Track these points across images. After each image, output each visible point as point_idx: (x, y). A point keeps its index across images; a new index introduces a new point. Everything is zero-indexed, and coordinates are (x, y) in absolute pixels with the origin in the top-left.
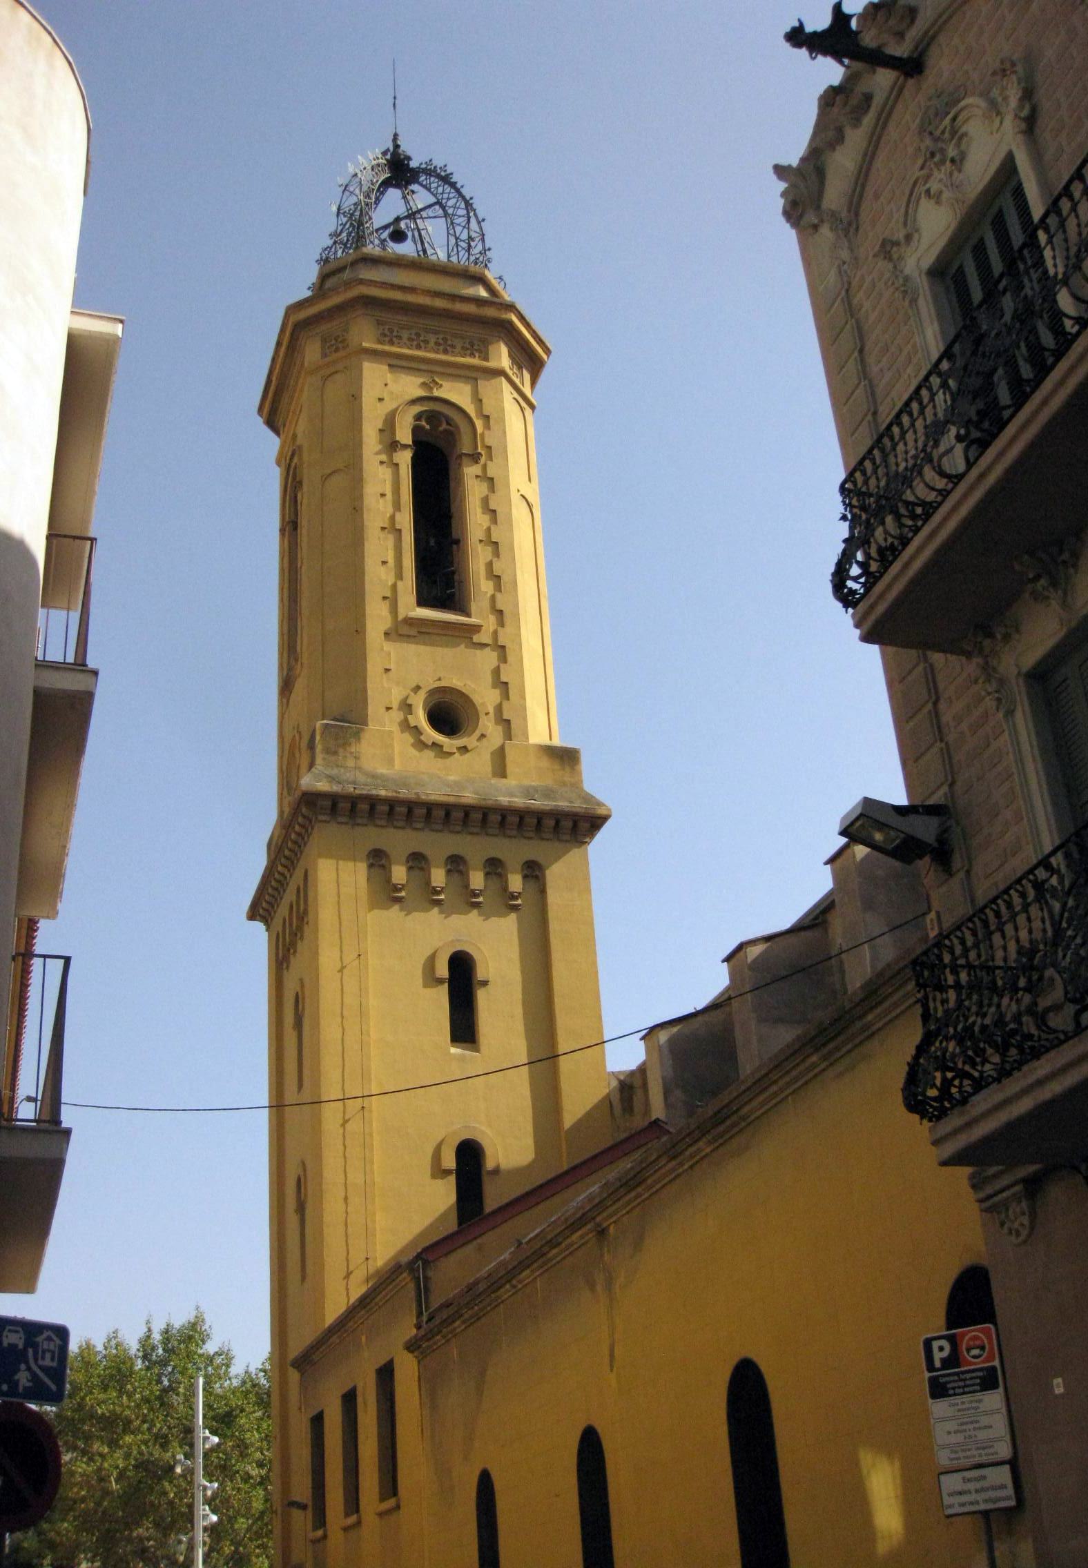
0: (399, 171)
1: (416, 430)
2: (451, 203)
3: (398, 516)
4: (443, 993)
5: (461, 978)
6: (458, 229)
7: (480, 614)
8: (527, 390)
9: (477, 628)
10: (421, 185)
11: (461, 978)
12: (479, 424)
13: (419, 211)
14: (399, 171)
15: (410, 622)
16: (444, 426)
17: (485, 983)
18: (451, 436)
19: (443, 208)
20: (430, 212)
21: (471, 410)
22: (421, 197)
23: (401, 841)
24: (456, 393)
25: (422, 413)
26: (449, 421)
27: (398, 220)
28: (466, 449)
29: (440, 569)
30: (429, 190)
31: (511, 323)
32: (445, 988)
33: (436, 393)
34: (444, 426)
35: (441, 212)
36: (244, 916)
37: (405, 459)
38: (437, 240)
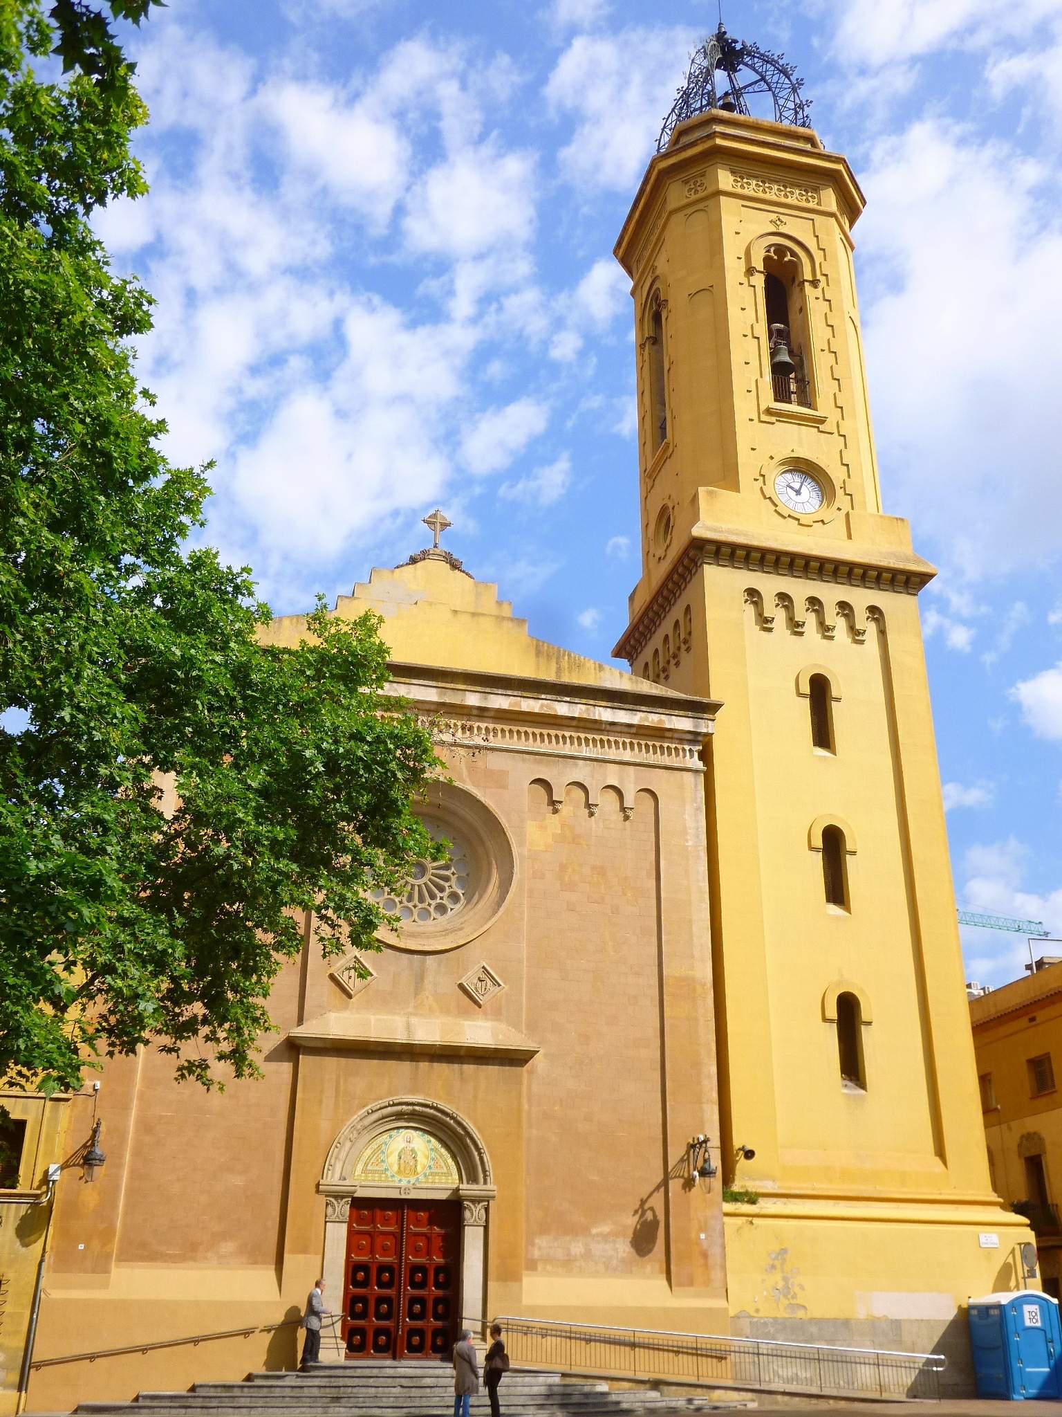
0: (728, 54)
1: (767, 260)
2: (775, 78)
3: (756, 327)
4: (806, 702)
5: (819, 693)
6: (781, 102)
7: (824, 406)
8: (847, 227)
9: (822, 421)
10: (746, 65)
11: (819, 693)
12: (818, 256)
13: (740, 89)
14: (728, 54)
15: (769, 412)
16: (788, 258)
17: (838, 700)
18: (795, 267)
19: (766, 82)
20: (756, 87)
21: (811, 244)
22: (745, 76)
23: (770, 584)
24: (796, 227)
25: (770, 246)
26: (793, 254)
27: (726, 94)
28: (808, 275)
29: (791, 375)
30: (754, 69)
31: (838, 171)
32: (807, 701)
33: (783, 229)
34: (788, 258)
35: (766, 87)
36: (610, 654)
37: (759, 280)
38: (760, 108)
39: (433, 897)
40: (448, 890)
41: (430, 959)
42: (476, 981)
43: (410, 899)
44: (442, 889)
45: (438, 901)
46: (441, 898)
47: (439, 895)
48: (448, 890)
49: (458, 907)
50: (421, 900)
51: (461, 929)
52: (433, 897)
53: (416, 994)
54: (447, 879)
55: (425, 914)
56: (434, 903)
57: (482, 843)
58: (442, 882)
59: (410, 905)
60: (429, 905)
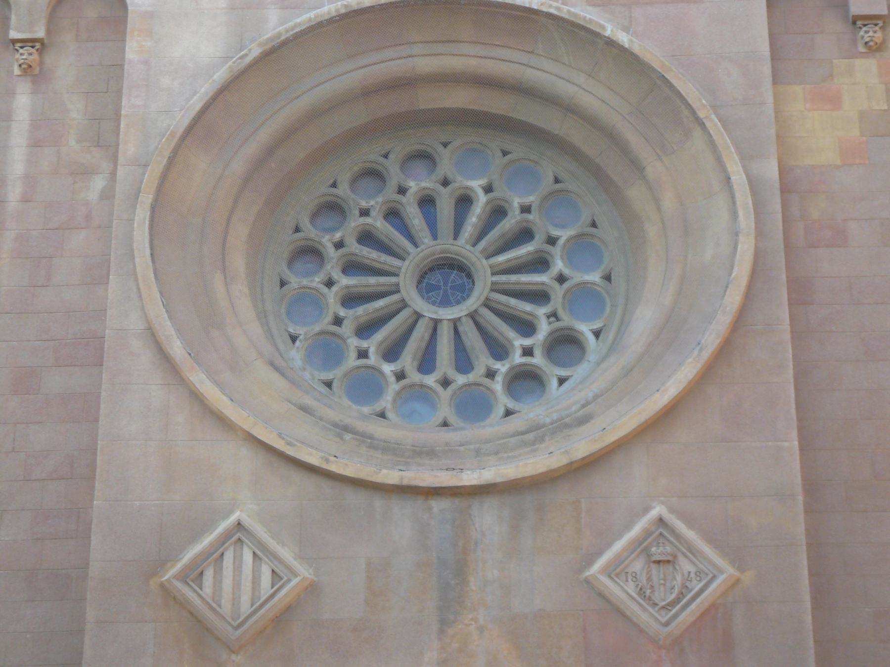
39: (499, 351)
40: (544, 329)
41: (488, 519)
42: (638, 566)
43: (426, 363)
44: (527, 327)
45: (518, 358)
46: (528, 352)
47: (519, 342)
48: (544, 329)
49: (578, 372)
50: (464, 363)
51: (583, 421)
52: (499, 351)
53: (444, 624)
54: (540, 296)
55: (473, 405)
56: (502, 368)
57: (637, 167)
58: (526, 307)
59: (430, 380)
60: (491, 374)
